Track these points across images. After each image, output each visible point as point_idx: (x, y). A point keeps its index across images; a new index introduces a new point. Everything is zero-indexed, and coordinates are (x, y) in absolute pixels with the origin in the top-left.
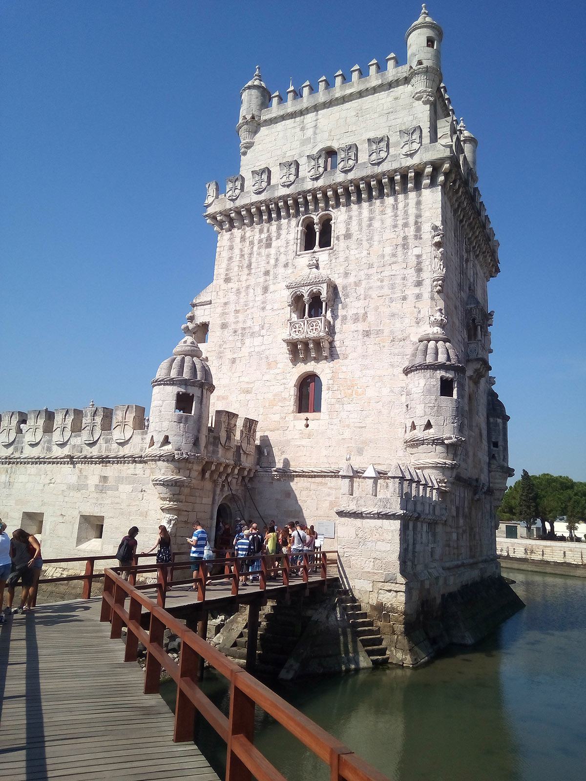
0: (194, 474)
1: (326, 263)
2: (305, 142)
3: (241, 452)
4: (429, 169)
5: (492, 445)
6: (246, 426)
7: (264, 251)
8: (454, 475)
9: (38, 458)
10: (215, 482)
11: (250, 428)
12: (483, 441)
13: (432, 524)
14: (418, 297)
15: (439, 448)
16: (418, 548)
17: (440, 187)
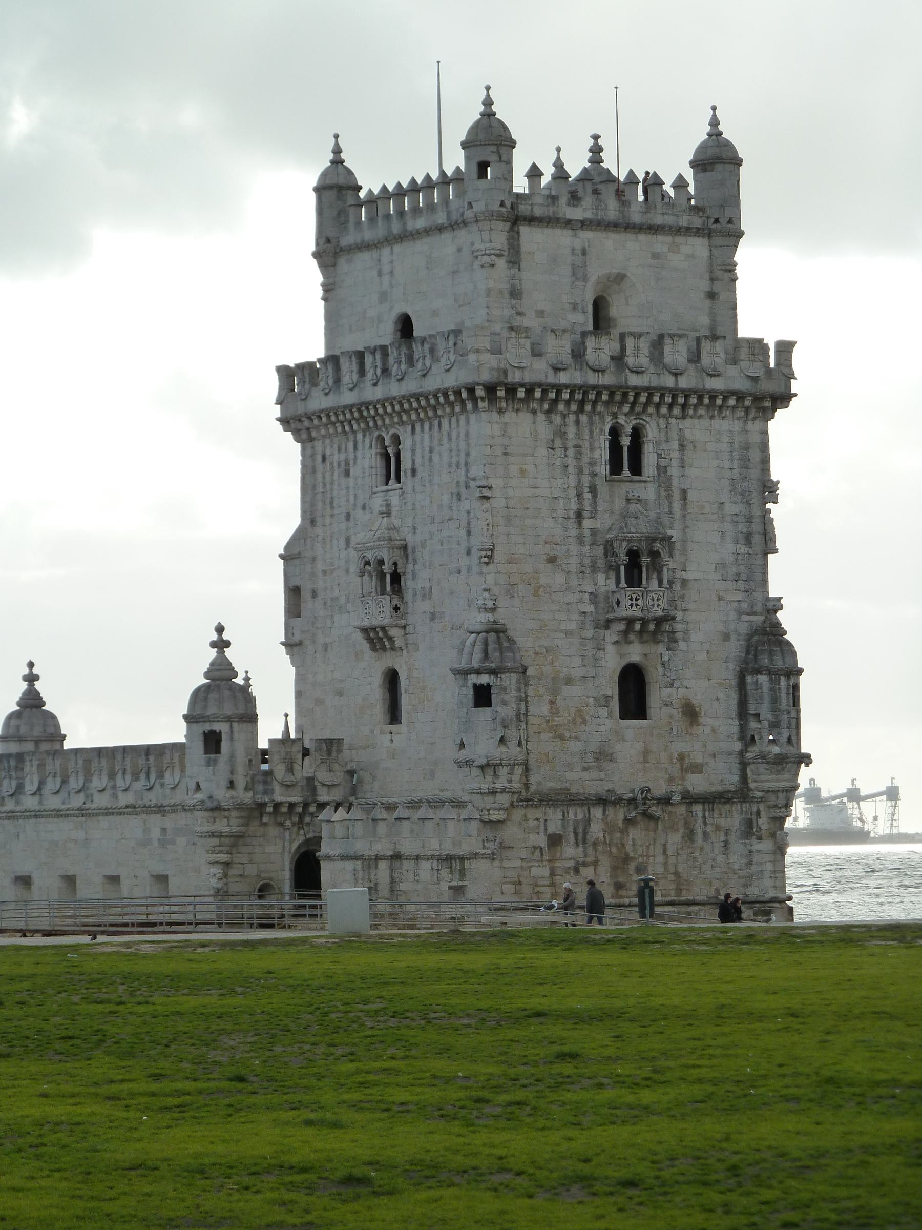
0: (234, 822)
1: (397, 509)
2: (383, 297)
3: (316, 783)
4: (464, 395)
5: (751, 719)
6: (321, 750)
7: (344, 481)
8: (504, 799)
9: (106, 809)
10: (281, 824)
11: (329, 752)
12: (701, 720)
14: (469, 569)
15: (475, 772)
16: (403, 887)
17: (483, 414)
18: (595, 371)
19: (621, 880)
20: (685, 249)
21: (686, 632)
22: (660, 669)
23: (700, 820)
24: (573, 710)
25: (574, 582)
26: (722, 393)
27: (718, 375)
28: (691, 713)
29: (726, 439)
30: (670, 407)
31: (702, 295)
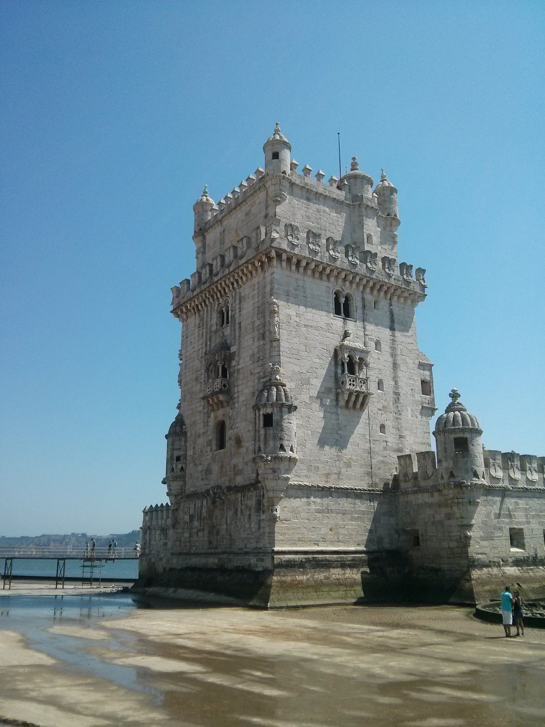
12: (243, 444)
13: (164, 530)
16: (152, 542)
18: (204, 284)
19: (211, 539)
20: (257, 202)
21: (238, 397)
22: (228, 420)
23: (240, 504)
24: (200, 450)
25: (202, 387)
26: (242, 265)
27: (243, 257)
28: (239, 442)
29: (256, 287)
30: (233, 284)
31: (263, 219)
